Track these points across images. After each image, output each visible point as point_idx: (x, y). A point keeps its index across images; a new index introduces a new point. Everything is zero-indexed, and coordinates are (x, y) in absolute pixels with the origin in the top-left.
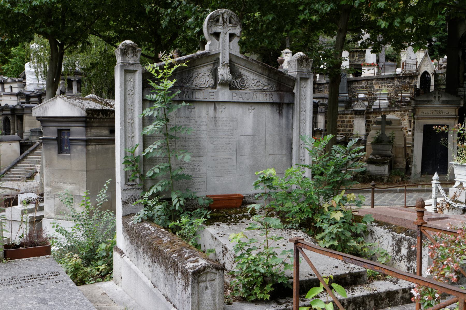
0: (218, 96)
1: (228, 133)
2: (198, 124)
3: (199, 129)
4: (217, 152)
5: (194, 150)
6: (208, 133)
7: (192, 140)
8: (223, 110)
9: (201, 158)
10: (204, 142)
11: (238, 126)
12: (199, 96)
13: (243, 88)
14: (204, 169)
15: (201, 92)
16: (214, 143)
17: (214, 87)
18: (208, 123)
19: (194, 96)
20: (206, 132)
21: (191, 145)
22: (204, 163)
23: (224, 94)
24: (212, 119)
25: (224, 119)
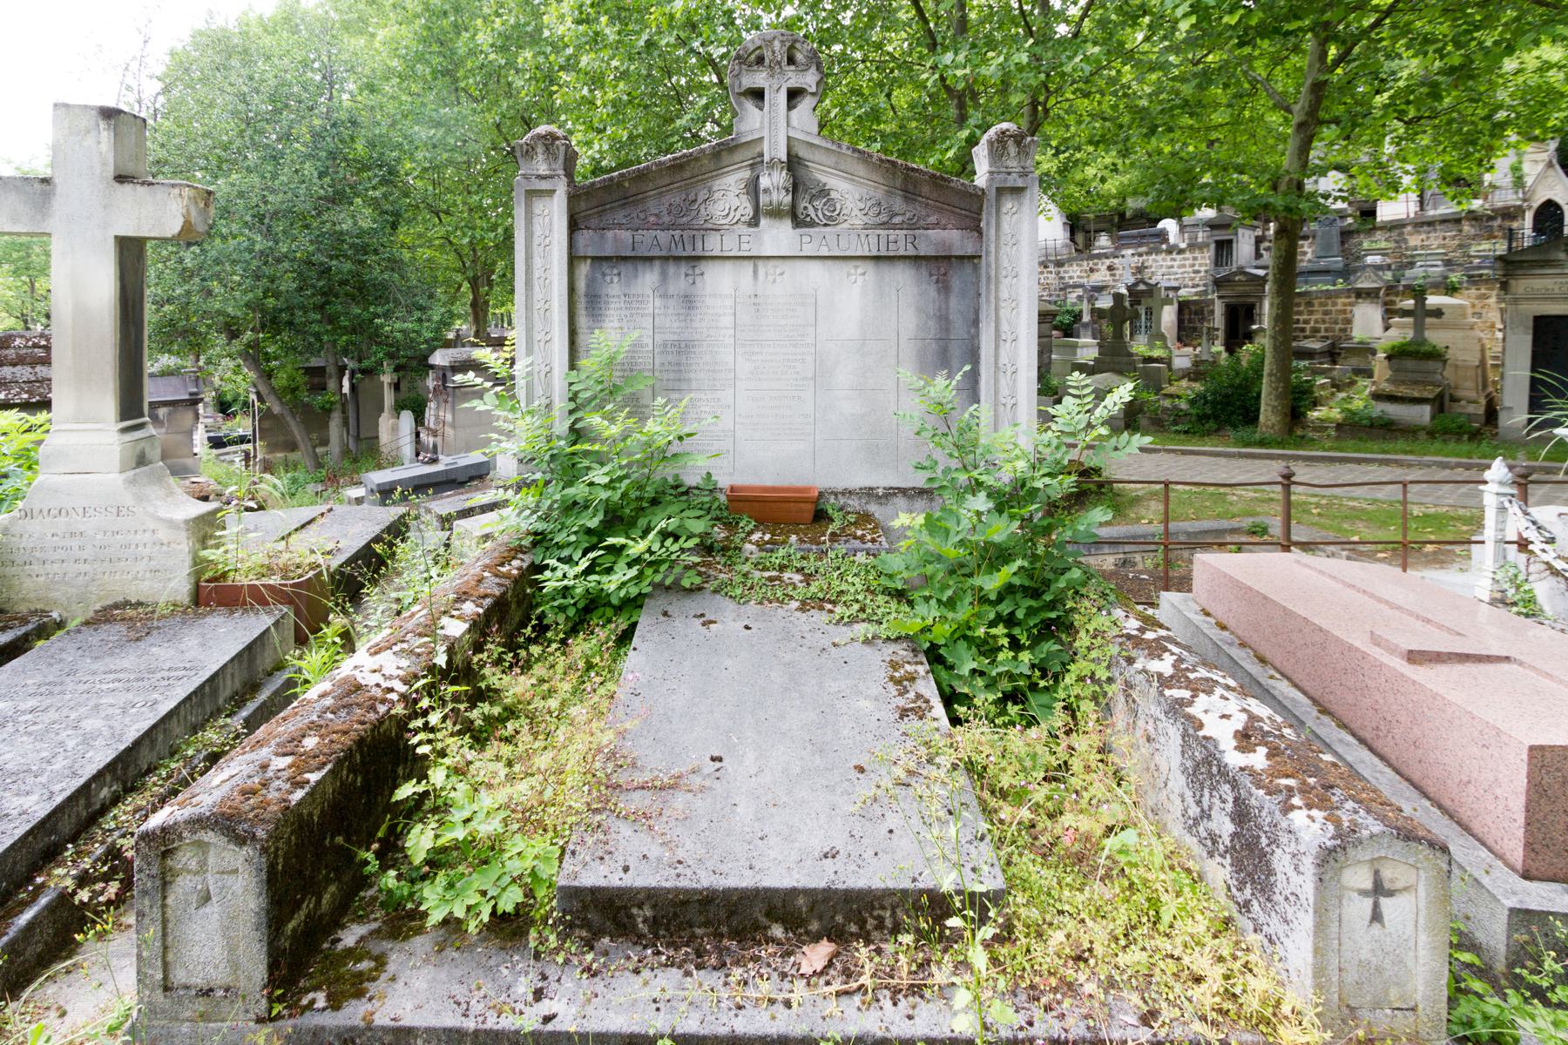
8: (779, 279)
12: (713, 245)
13: (831, 221)
15: (718, 234)
17: (754, 222)
19: (699, 245)
23: (778, 237)
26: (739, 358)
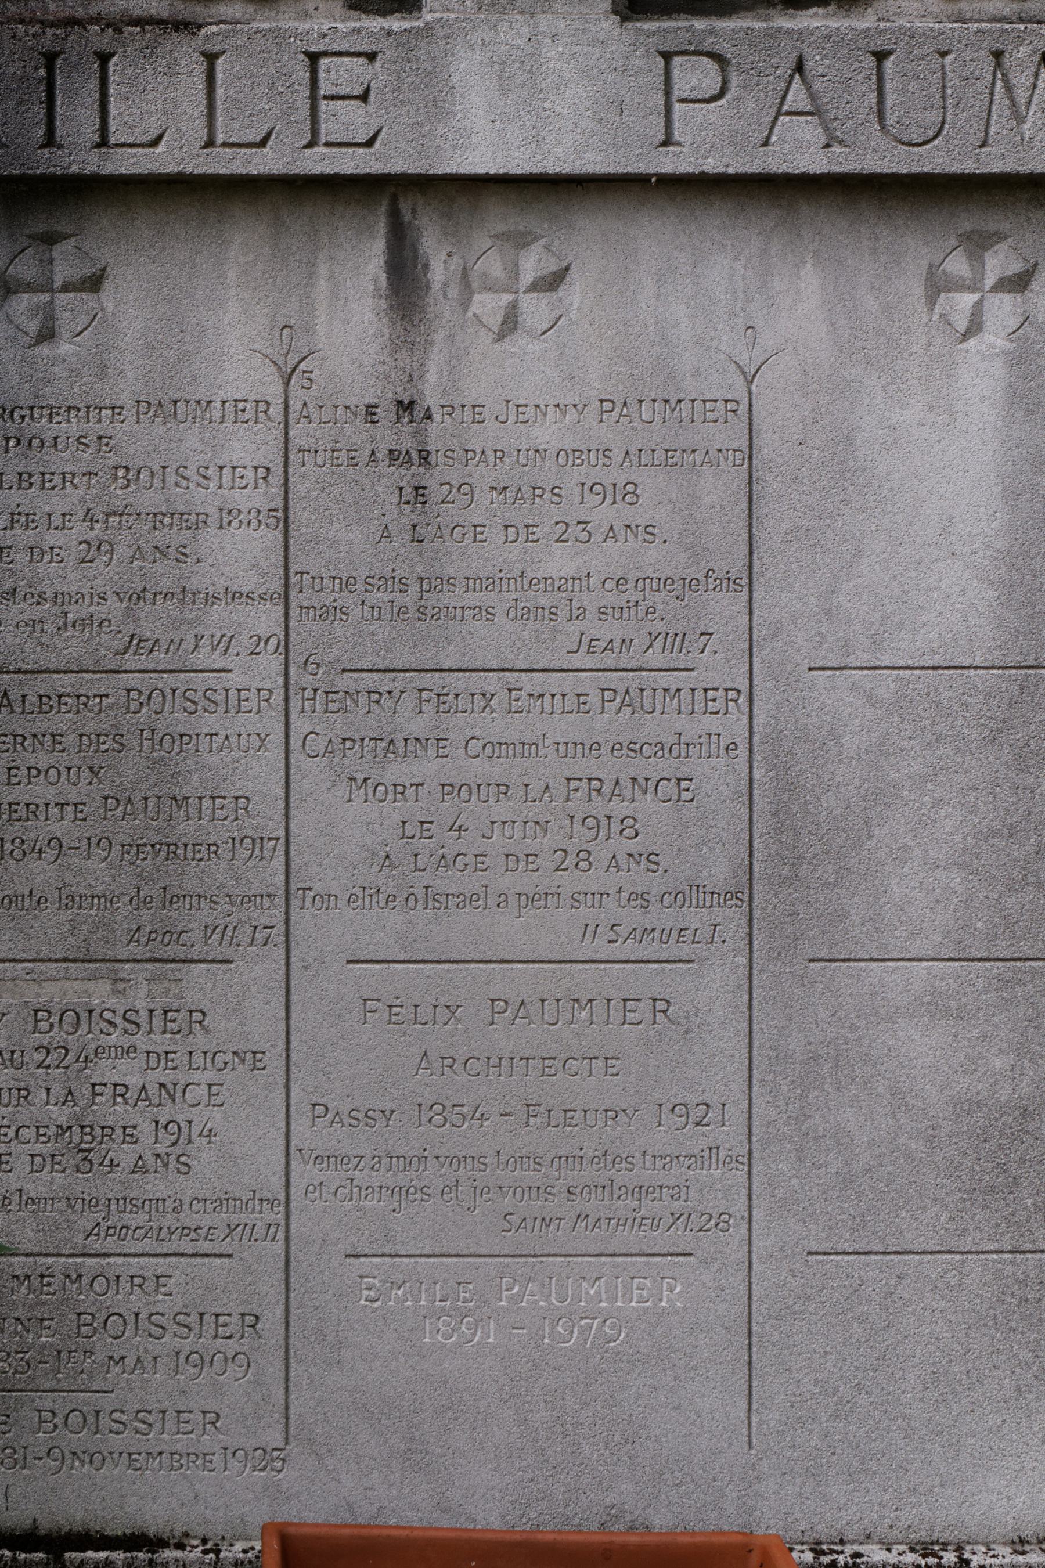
0: (435, 99)
1: (609, 630)
2: (150, 500)
3: (165, 575)
4: (431, 898)
5: (97, 872)
6: (304, 629)
7: (62, 721)
8: (536, 309)
9: (198, 985)
10: (242, 762)
11: (771, 533)
14: (240, 1141)
15: (186, 55)
16: (397, 771)
18: (299, 487)
19: (77, 118)
20: (266, 619)
21: (41, 791)
24: (356, 433)
25: (547, 434)
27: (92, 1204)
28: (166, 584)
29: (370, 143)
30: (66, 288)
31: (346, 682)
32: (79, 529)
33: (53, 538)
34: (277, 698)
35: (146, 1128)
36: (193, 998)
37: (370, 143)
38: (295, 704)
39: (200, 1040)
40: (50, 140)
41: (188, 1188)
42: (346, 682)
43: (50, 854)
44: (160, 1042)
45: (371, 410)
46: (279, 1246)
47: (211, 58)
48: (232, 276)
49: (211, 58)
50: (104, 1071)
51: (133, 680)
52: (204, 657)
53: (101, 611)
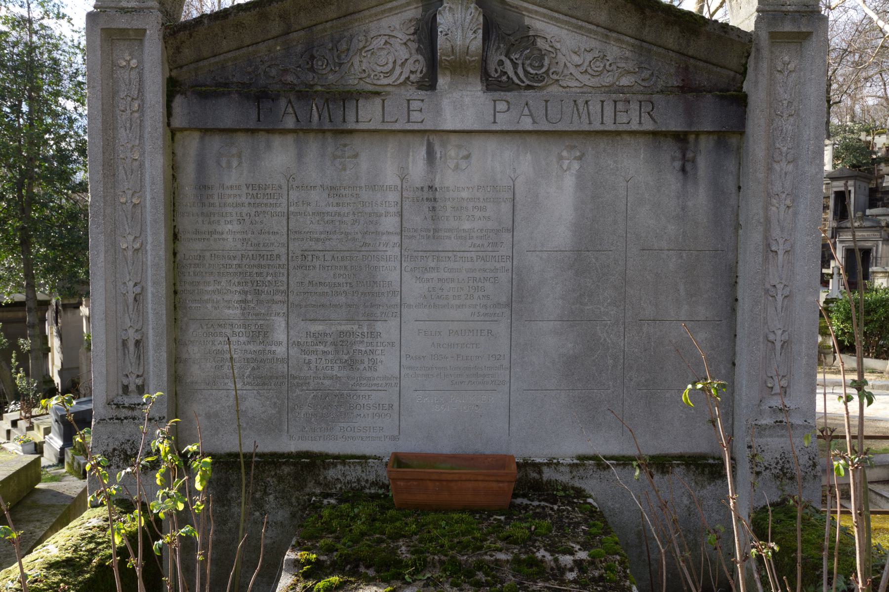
0: (438, 112)
1: (478, 242)
2: (368, 210)
4: (435, 306)
6: (406, 241)
8: (463, 164)
9: (379, 326)
11: (518, 218)
12: (369, 114)
13: (535, 83)
14: (388, 363)
15: (378, 101)
16: (428, 275)
17: (428, 83)
18: (405, 207)
19: (351, 116)
20: (396, 239)
22: (392, 344)
23: (462, 104)
24: (419, 193)
25: (465, 195)
26: (407, 276)
27: (353, 379)
28: (373, 230)
29: (422, 122)
30: (348, 158)
31: (415, 254)
32: (351, 217)
33: (345, 219)
34: (399, 258)
35: (366, 360)
36: (378, 329)
37: (422, 122)
38: (403, 259)
39: (379, 340)
40: (344, 121)
41: (376, 374)
42: (415, 254)
43: (344, 295)
44: (370, 340)
45: (422, 188)
46: (398, 388)
47: (383, 101)
48: (389, 155)
49: (383, 101)
50: (356, 347)
51: (364, 253)
52: (382, 248)
53: (356, 237)
